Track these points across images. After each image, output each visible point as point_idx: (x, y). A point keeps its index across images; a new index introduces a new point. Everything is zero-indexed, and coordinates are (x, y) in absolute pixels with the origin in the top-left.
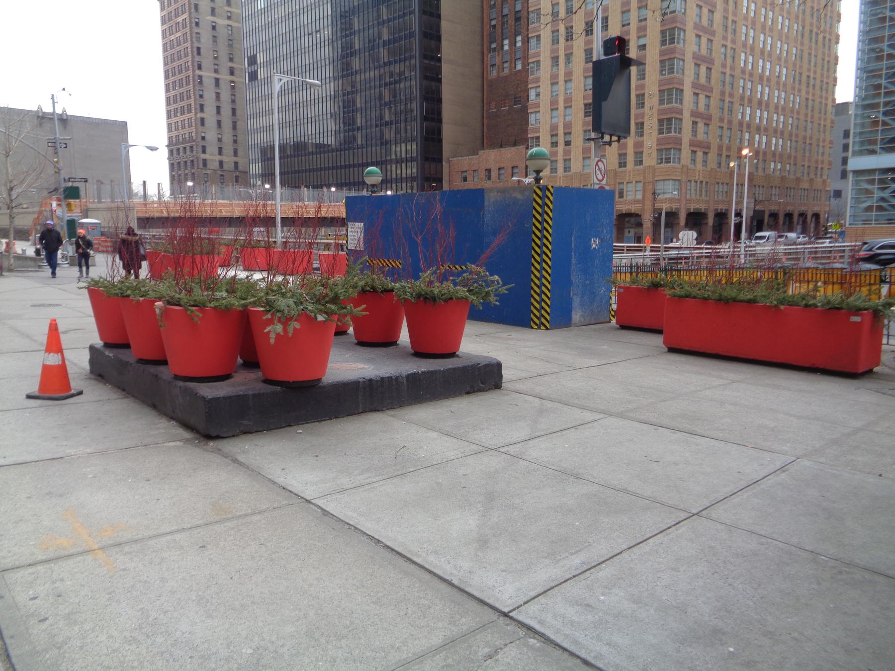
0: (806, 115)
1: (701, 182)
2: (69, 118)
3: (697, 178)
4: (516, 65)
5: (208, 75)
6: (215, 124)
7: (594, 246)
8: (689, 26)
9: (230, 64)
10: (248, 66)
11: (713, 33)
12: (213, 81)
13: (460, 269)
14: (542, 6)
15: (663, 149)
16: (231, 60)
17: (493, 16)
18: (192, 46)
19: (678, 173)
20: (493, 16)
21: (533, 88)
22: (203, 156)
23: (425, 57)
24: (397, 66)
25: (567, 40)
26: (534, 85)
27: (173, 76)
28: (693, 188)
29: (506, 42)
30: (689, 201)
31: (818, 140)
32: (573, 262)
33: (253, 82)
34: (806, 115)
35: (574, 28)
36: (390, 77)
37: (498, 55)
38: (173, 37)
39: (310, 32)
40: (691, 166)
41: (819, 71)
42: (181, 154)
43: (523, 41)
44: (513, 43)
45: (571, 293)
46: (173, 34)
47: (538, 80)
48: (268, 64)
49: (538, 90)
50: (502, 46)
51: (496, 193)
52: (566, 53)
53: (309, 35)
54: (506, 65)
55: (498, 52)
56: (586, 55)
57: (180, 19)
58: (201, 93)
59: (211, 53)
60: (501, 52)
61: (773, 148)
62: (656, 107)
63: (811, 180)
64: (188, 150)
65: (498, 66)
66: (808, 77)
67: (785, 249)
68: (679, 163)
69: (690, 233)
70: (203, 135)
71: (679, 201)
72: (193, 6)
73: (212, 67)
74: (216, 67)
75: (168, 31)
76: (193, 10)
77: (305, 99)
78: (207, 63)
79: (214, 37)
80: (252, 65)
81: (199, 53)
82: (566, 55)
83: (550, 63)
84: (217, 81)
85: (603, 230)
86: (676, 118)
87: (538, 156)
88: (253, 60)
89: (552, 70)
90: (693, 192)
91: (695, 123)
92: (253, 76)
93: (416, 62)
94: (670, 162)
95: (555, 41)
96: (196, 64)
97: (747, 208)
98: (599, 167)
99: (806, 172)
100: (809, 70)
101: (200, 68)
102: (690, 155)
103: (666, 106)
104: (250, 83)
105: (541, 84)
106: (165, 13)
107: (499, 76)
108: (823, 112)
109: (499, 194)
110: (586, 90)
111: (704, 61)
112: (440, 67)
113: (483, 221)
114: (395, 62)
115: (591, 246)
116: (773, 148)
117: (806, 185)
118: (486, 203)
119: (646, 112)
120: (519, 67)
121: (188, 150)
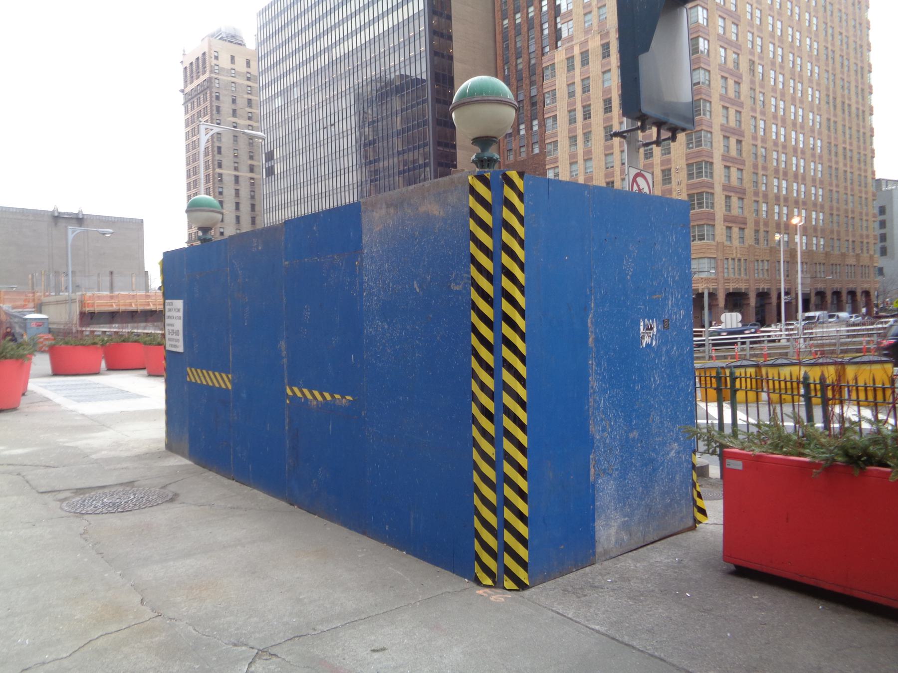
0: (846, 188)
1: (739, 260)
2: (85, 217)
3: (734, 255)
4: (533, 149)
5: (228, 173)
6: (234, 220)
7: (647, 340)
8: (715, 98)
9: (250, 162)
10: (266, 162)
11: (741, 105)
12: (233, 178)
13: (320, 398)
14: (557, 87)
15: (695, 226)
16: (251, 158)
19: (712, 251)
21: (551, 168)
23: (439, 144)
24: (411, 154)
25: (585, 119)
26: (552, 166)
27: (194, 175)
28: (731, 267)
29: (522, 127)
30: (727, 281)
31: (861, 213)
32: (594, 384)
33: (270, 177)
34: (846, 188)
35: (592, 107)
36: (404, 166)
37: (515, 139)
39: (325, 126)
40: (727, 243)
41: (855, 143)
43: (540, 125)
44: (530, 128)
45: (592, 470)
46: (195, 135)
47: (556, 160)
48: (284, 158)
49: (556, 170)
50: (519, 131)
51: (383, 211)
52: (585, 131)
53: (324, 128)
54: (523, 149)
55: (515, 137)
56: (604, 50)
58: (220, 190)
59: (232, 151)
60: (517, 137)
61: (814, 223)
62: (685, 182)
63: (858, 256)
65: (515, 151)
66: (845, 149)
67: (848, 331)
68: (714, 239)
69: (734, 314)
70: (222, 230)
71: (716, 280)
72: (214, 108)
73: (232, 165)
74: (236, 165)
75: (190, 133)
76: (214, 112)
77: (320, 192)
78: (227, 161)
79: (234, 136)
80: (269, 161)
81: (219, 152)
82: (584, 134)
83: (568, 143)
84: (237, 178)
85: (666, 298)
86: (707, 193)
87: (481, 93)
88: (270, 156)
89: (570, 150)
90: (731, 271)
91: (728, 198)
92: (270, 171)
93: (430, 149)
94: (704, 239)
95: (572, 120)
96: (216, 163)
97: (802, 284)
98: (638, 186)
99: (851, 247)
100: (844, 142)
101: (220, 166)
102: (724, 231)
103: (695, 180)
104: (267, 178)
105: (559, 164)
106: (188, 116)
107: (516, 160)
108: (863, 184)
109: (392, 211)
110: (607, 168)
111: (734, 134)
112: (455, 154)
113: (362, 283)
114: (409, 150)
115: (638, 339)
116: (814, 223)
117: (851, 261)
118: (366, 239)
119: (674, 187)
120: (536, 151)
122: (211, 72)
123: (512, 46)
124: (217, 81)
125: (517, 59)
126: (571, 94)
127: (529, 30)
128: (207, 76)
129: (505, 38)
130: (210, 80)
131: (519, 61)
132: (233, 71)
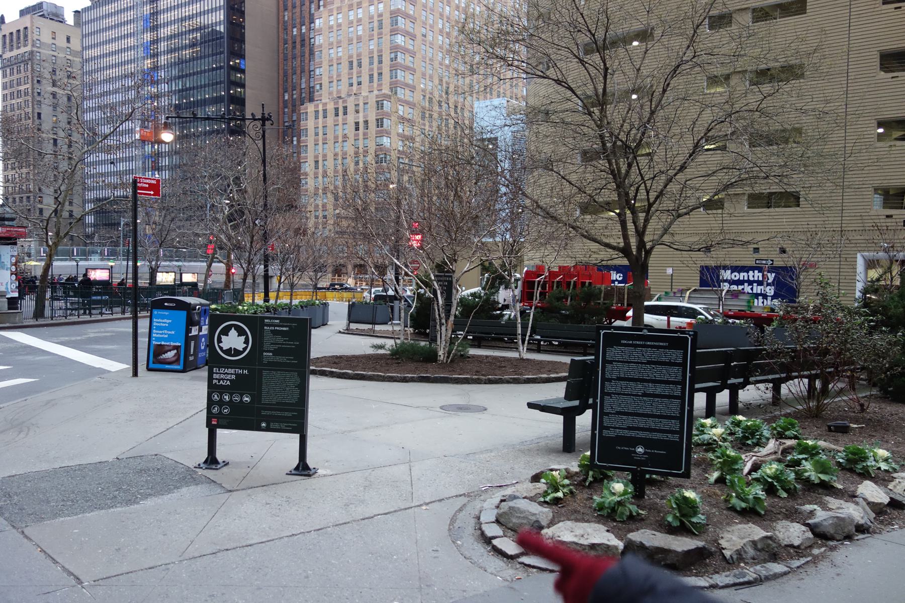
17: (286, 120)
18: (33, 112)
20: (286, 120)
22: (40, 206)
38: (13, 102)
42: (17, 204)
54: (295, 155)
57: (22, 88)
64: (25, 199)
121: (25, 199)
122: (33, 46)
123: (289, 80)
124: (38, 54)
125: (293, 90)
126: (317, 134)
127: (301, 73)
128: (28, 48)
129: (285, 75)
130: (32, 53)
131: (294, 92)
132: (54, 46)
